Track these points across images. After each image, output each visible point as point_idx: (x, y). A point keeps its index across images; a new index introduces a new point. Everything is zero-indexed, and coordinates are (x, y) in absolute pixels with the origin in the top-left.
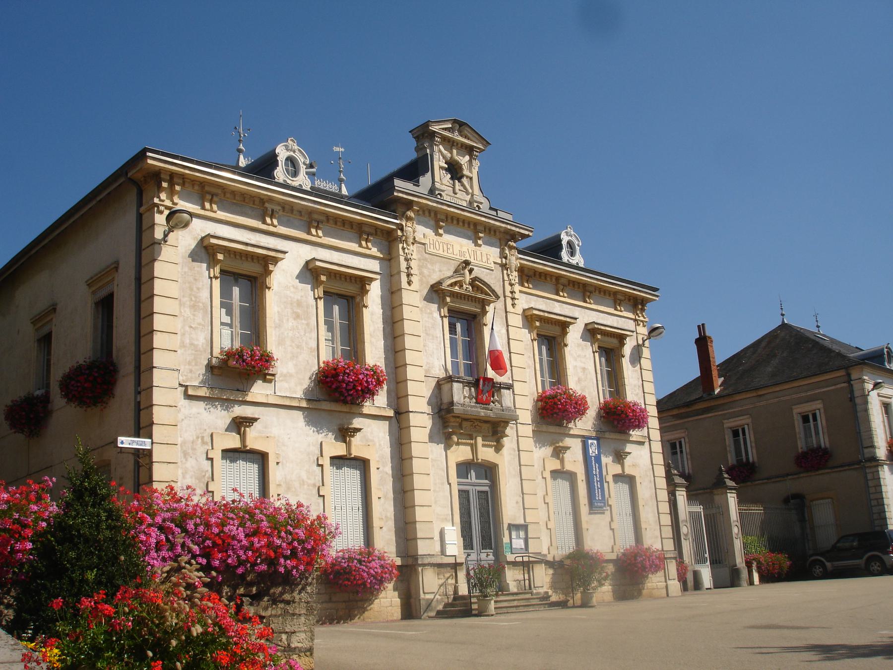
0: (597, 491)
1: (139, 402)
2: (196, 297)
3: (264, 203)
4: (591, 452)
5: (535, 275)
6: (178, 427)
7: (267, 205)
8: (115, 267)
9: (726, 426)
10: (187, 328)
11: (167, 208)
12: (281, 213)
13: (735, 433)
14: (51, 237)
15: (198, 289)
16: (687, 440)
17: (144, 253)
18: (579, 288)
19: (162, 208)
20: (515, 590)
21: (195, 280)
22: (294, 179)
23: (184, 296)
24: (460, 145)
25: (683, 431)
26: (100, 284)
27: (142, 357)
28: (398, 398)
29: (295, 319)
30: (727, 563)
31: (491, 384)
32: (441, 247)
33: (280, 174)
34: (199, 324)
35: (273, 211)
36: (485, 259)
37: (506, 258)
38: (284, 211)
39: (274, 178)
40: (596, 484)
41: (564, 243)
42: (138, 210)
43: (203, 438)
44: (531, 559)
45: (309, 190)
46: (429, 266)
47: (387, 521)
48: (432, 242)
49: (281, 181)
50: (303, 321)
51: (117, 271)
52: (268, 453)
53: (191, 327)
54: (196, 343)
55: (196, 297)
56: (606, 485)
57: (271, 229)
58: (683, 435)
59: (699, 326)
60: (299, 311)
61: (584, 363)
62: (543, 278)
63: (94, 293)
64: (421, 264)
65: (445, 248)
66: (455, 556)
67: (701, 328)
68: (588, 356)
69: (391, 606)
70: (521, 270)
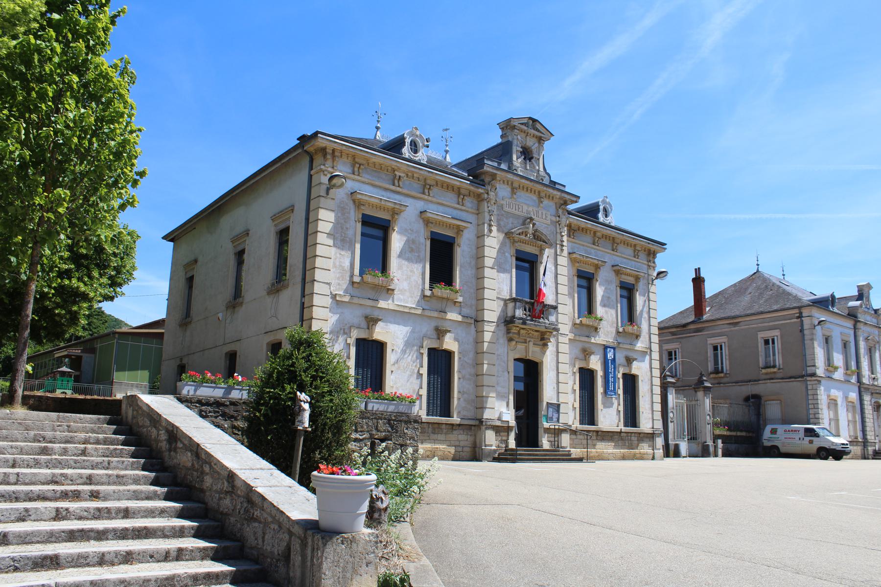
1: (304, 303)
2: (345, 234)
3: (394, 171)
4: (609, 357)
5: (579, 230)
6: (329, 321)
7: (396, 173)
8: (292, 209)
9: (709, 342)
10: (338, 255)
11: (329, 172)
12: (405, 178)
13: (715, 348)
14: (248, 185)
15: (347, 228)
16: (680, 350)
17: (312, 202)
18: (609, 240)
19: (326, 173)
20: (548, 448)
21: (345, 222)
23: (337, 233)
24: (532, 135)
25: (678, 343)
26: (280, 220)
27: (307, 272)
28: (477, 311)
29: (410, 252)
30: (700, 440)
31: (542, 305)
32: (514, 207)
33: (406, 151)
35: (400, 177)
36: (544, 217)
37: (559, 217)
38: (407, 177)
39: (402, 154)
41: (601, 208)
42: (309, 172)
43: (344, 330)
44: (560, 427)
45: (425, 163)
46: (505, 219)
47: (463, 394)
49: (407, 157)
50: (416, 254)
51: (293, 212)
52: (386, 343)
54: (343, 265)
55: (345, 234)
56: (617, 379)
57: (398, 189)
58: (677, 346)
59: (696, 269)
60: (413, 246)
62: (584, 231)
63: (276, 225)
66: (508, 421)
67: (698, 271)
68: (612, 289)
70: (569, 226)
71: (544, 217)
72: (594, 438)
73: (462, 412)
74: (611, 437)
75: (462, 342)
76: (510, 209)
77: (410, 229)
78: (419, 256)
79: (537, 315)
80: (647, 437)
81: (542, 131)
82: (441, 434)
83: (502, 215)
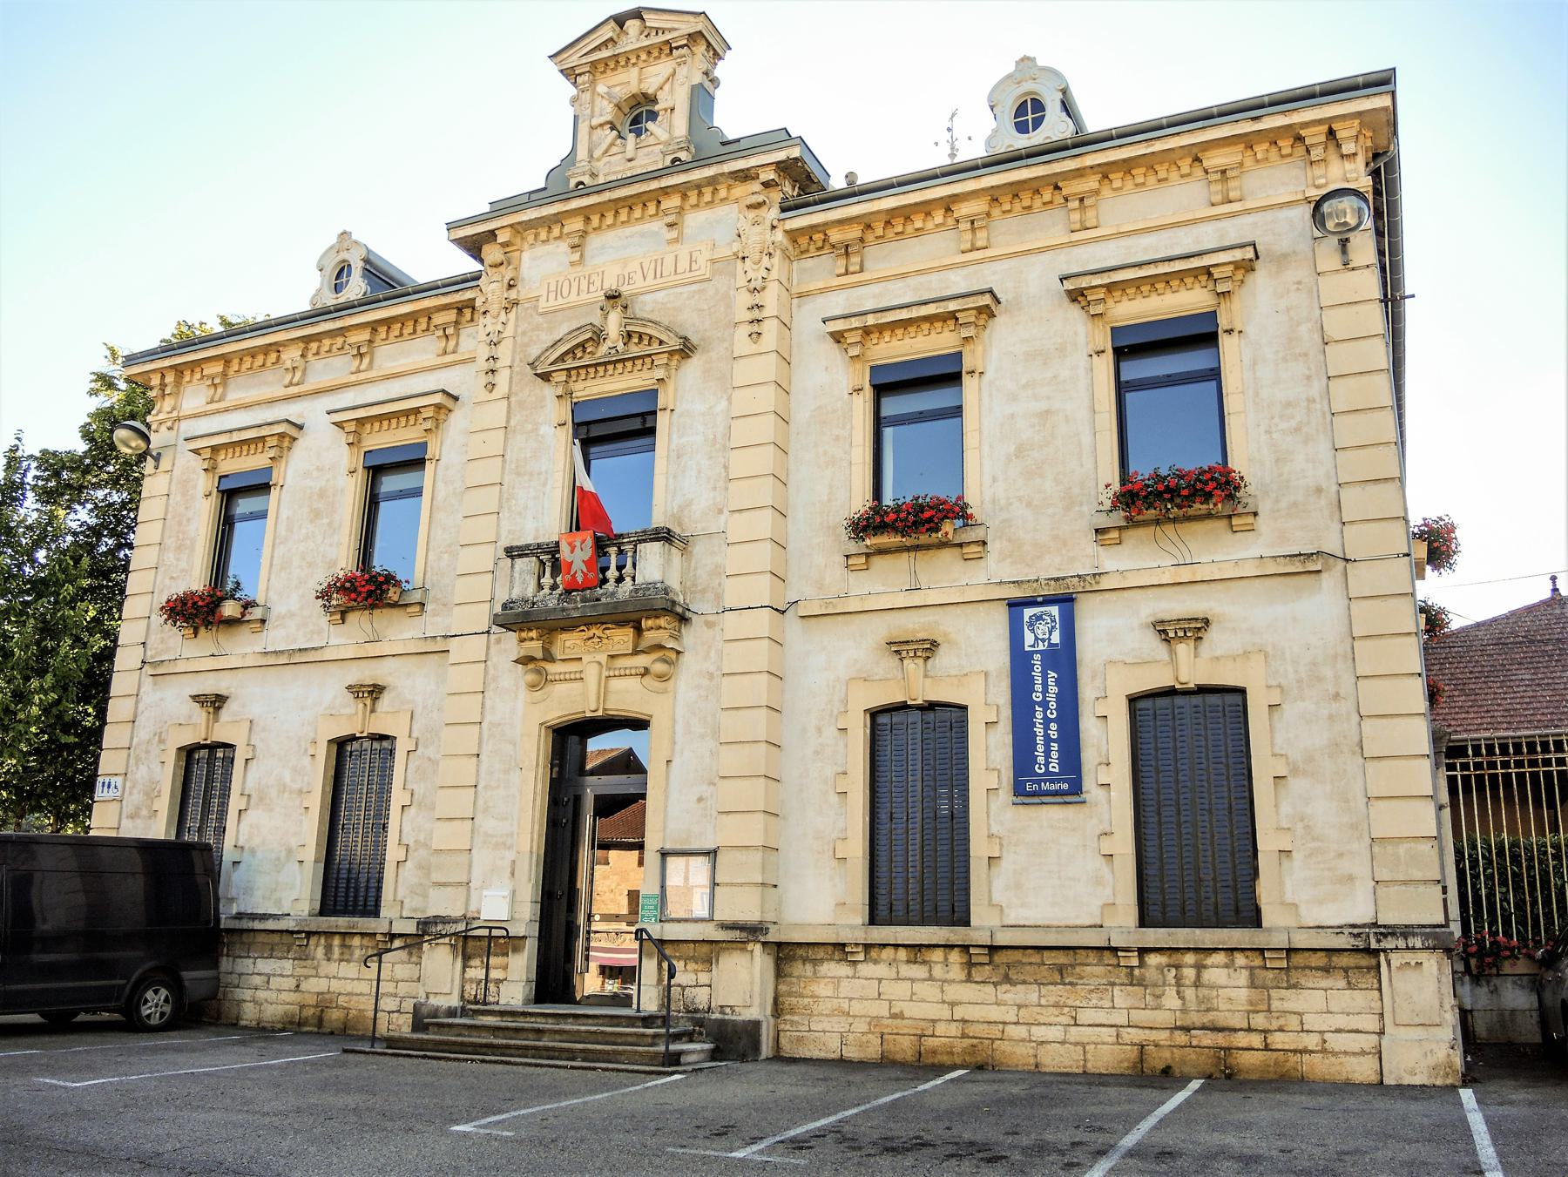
0: (1040, 748)
22: (338, 295)
34: (182, 571)
40: (1039, 730)
47: (416, 850)
48: (553, 288)
53: (172, 578)
61: (1049, 398)
64: (526, 340)
65: (584, 286)
69: (398, 1011)
71: (683, 264)
72: (957, 972)
73: (406, 901)
74: (1061, 969)
75: (425, 707)
76: (560, 301)
77: (318, 469)
78: (330, 524)
79: (580, 579)
80: (1327, 970)
81: (668, 25)
82: (348, 961)
83: (537, 328)
